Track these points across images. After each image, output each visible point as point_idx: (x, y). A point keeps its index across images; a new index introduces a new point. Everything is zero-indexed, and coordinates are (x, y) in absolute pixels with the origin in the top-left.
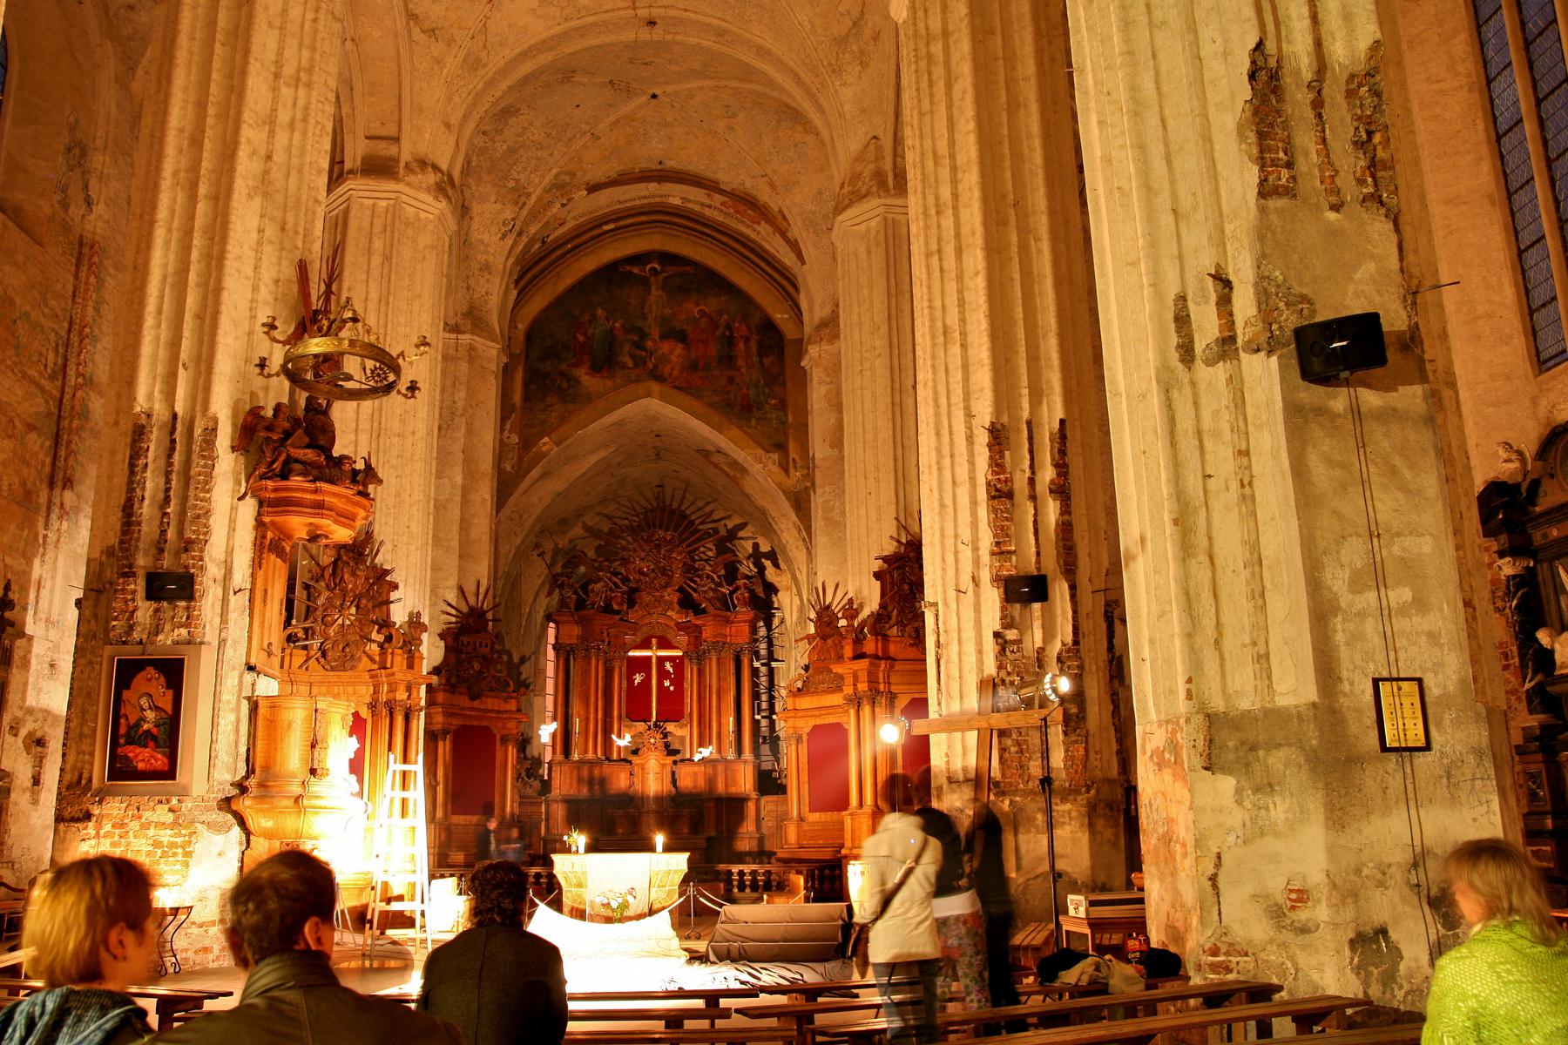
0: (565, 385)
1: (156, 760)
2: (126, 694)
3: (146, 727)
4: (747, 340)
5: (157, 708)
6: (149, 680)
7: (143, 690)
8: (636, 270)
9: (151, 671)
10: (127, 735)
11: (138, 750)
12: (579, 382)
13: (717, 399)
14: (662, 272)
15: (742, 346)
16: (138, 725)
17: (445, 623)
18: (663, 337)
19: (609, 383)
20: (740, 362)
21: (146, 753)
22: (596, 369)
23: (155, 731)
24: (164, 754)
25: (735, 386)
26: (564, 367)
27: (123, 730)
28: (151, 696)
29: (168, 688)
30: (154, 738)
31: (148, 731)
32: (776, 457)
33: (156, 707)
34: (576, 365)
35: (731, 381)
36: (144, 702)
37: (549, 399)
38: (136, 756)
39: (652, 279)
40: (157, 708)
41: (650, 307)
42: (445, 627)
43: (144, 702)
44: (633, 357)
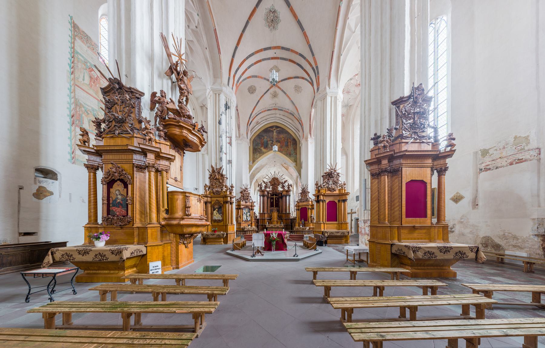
1: (122, 212)
2: (111, 190)
3: (118, 201)
4: (290, 142)
5: (122, 195)
6: (118, 185)
7: (117, 189)
9: (118, 182)
10: (113, 203)
11: (116, 209)
15: (289, 143)
16: (116, 200)
18: (276, 142)
19: (267, 150)
21: (119, 209)
22: (265, 148)
23: (121, 202)
24: (125, 210)
26: (259, 147)
27: (111, 202)
28: (119, 190)
29: (125, 188)
30: (121, 204)
31: (119, 202)
33: (121, 194)
34: (261, 147)
35: (288, 150)
36: (117, 192)
38: (116, 210)
40: (122, 195)
43: (117, 192)
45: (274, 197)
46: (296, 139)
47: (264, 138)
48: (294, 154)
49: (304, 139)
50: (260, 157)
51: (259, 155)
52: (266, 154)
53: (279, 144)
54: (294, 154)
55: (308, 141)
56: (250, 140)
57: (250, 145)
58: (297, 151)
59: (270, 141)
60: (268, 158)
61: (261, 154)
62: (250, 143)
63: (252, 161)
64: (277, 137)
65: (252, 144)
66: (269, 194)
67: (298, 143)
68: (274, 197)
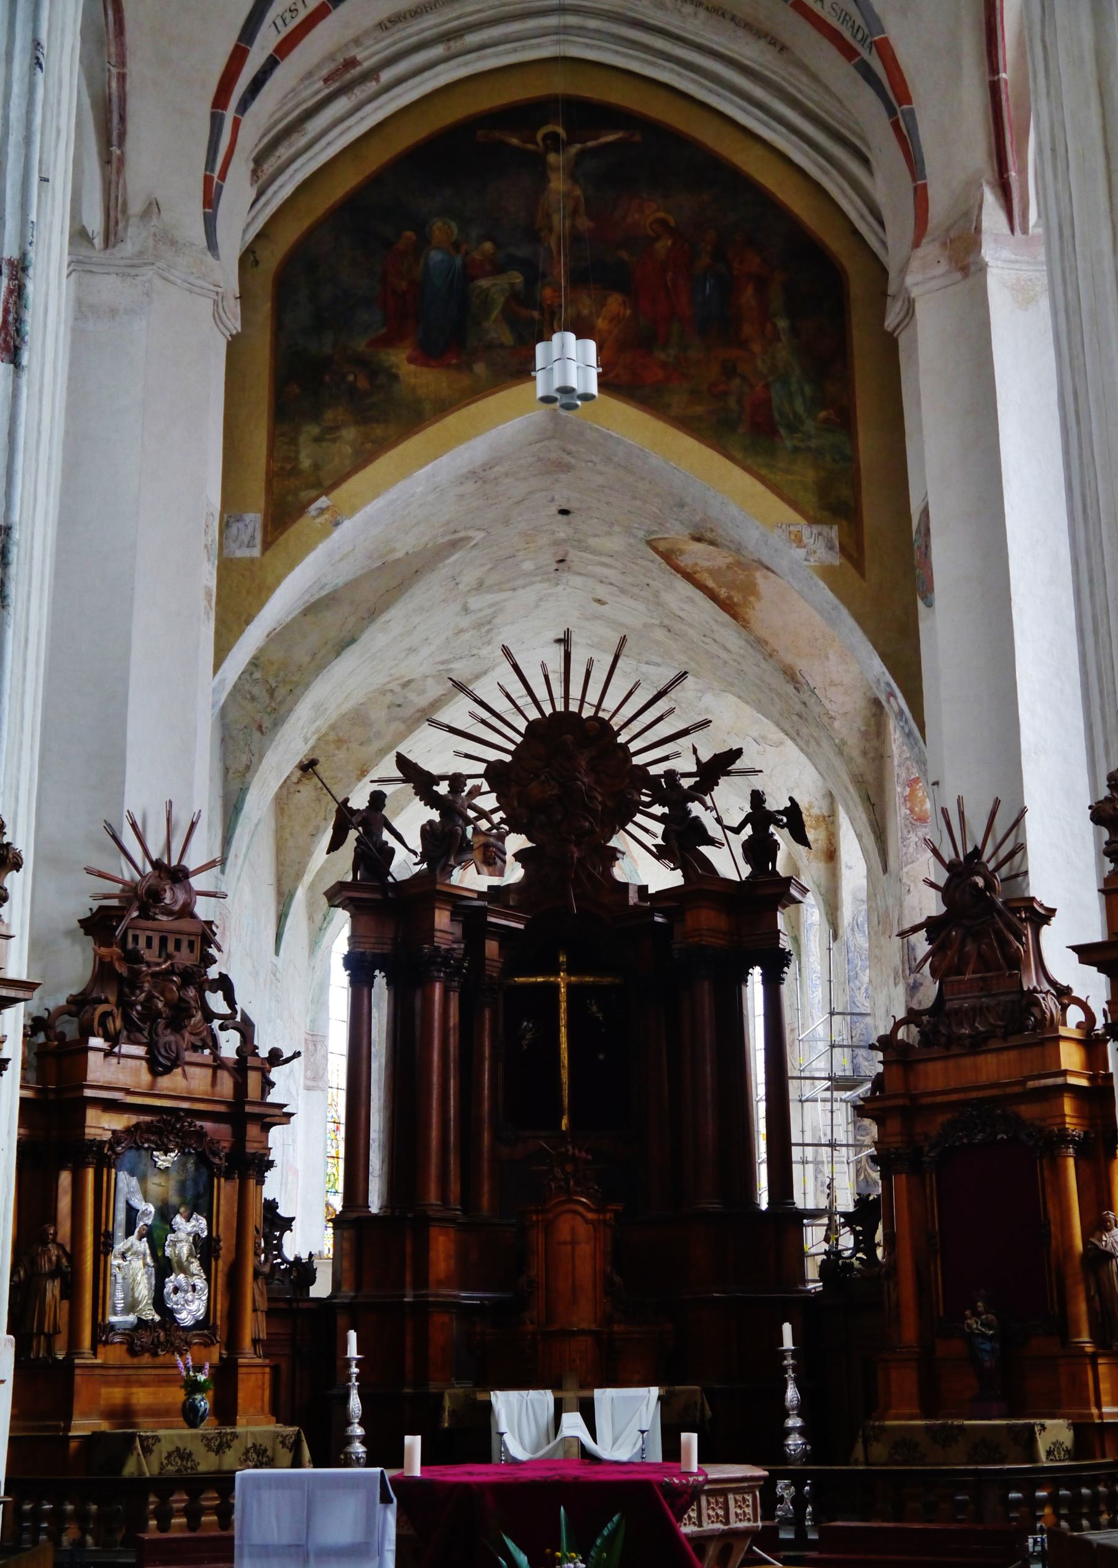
0: (363, 384)
8: (515, 141)
12: (395, 377)
13: (699, 409)
14: (570, 142)
15: (748, 296)
17: (95, 897)
18: (578, 279)
19: (466, 381)
20: (748, 330)
25: (737, 381)
26: (360, 345)
32: (834, 532)
34: (389, 341)
35: (729, 371)
37: (329, 415)
39: (552, 158)
41: (548, 216)
42: (95, 905)
44: (510, 318)
45: (562, 980)
46: (836, 244)
47: (424, 241)
48: (809, 425)
49: (929, 249)
50: (363, 459)
51: (349, 433)
52: (452, 421)
53: (615, 303)
54: (809, 425)
55: (983, 268)
56: (248, 259)
57: (236, 326)
58: (848, 383)
59: (499, 269)
60: (480, 475)
61: (379, 431)
62: (244, 296)
63: (254, 520)
64: (584, 223)
65: (266, 307)
66: (492, 947)
67: (857, 288)
68: (562, 980)
